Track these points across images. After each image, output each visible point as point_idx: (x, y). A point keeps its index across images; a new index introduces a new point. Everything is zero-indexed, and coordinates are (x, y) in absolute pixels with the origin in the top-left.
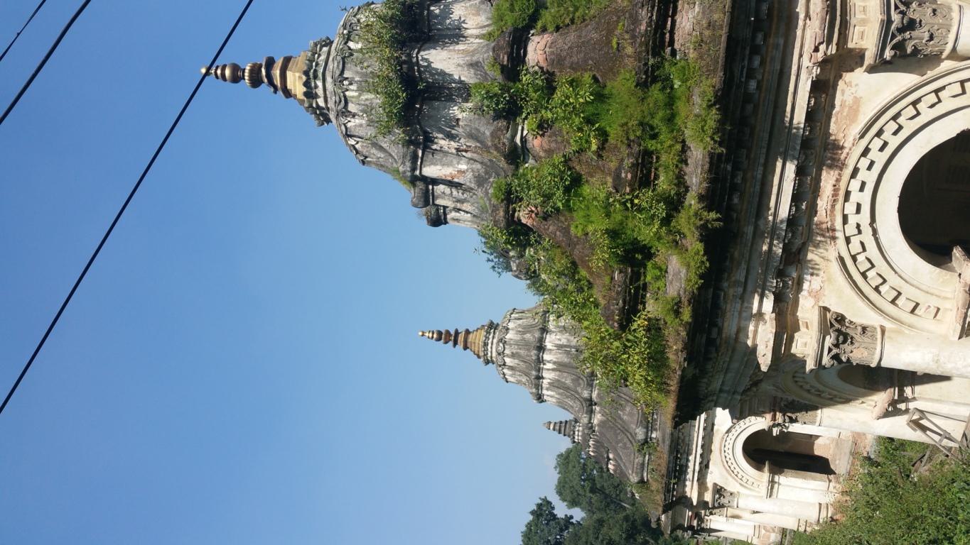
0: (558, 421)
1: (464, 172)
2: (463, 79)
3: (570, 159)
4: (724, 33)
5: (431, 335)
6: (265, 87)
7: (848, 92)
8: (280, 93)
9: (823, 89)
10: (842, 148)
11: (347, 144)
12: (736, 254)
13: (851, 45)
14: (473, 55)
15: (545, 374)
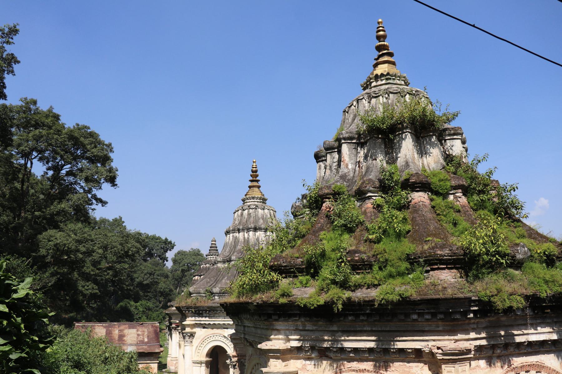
0: (217, 245)
1: (347, 167)
2: (399, 159)
3: (362, 225)
4: (441, 296)
6: (376, 54)
8: (375, 62)
10: (386, 371)
11: (353, 101)
12: (320, 323)
14: (412, 163)
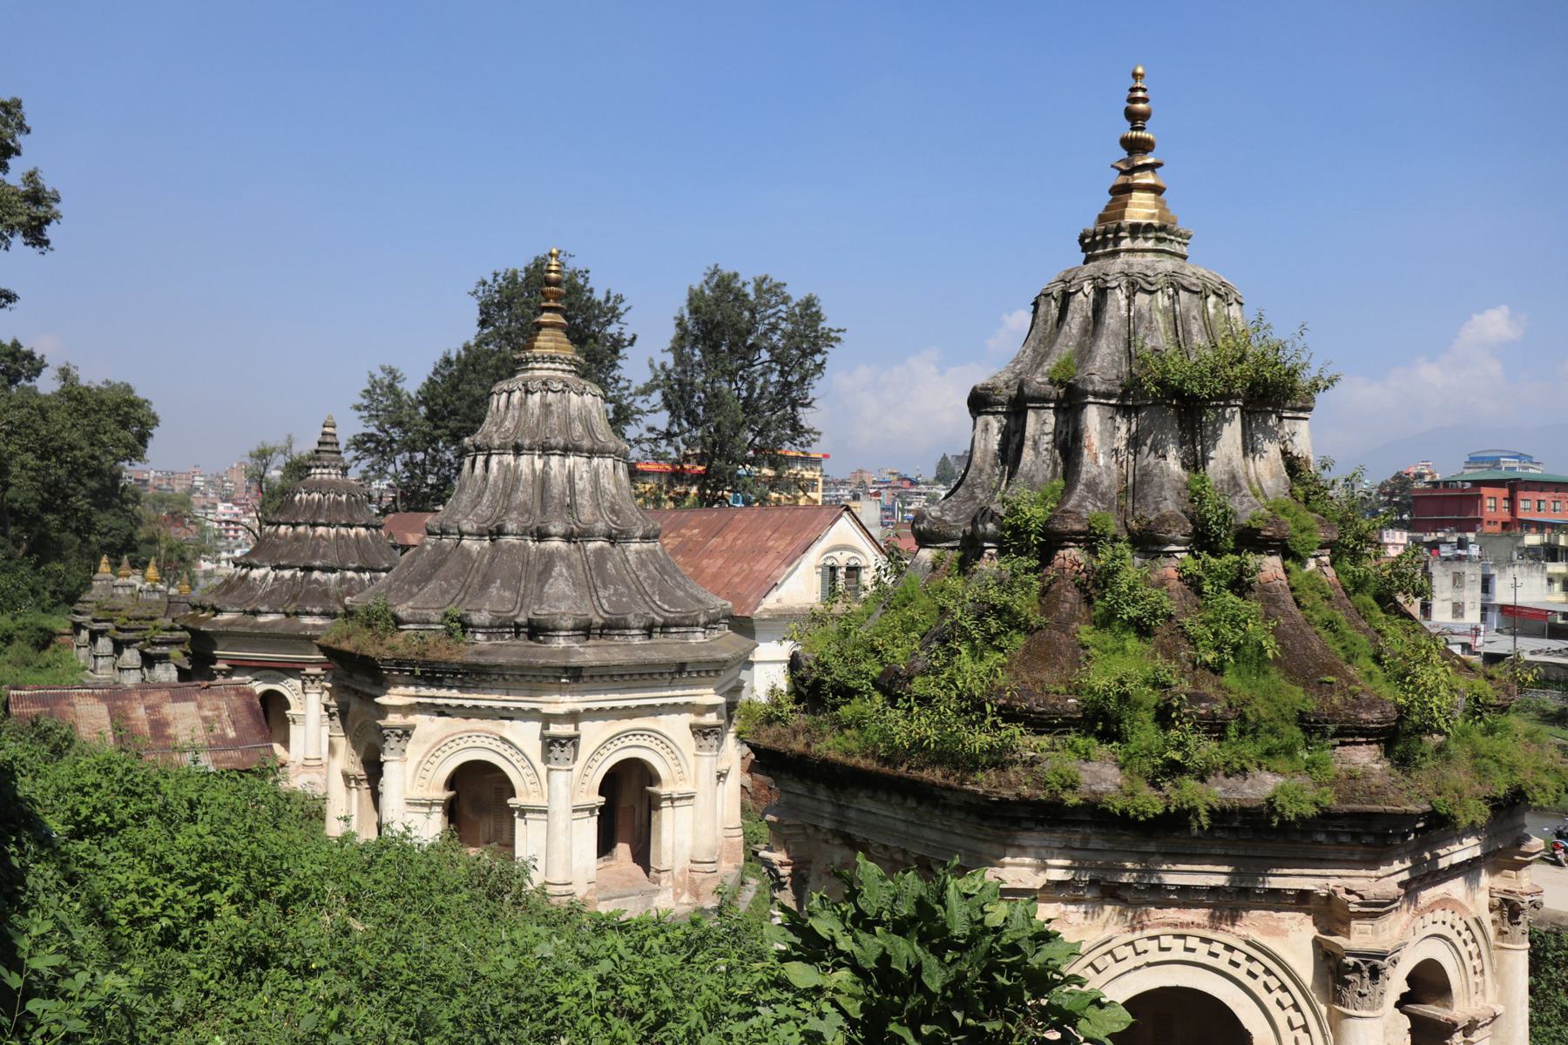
7: (1292, 923)
8: (1121, 180)
9: (1302, 900)
13: (1353, 923)
15: (524, 460)
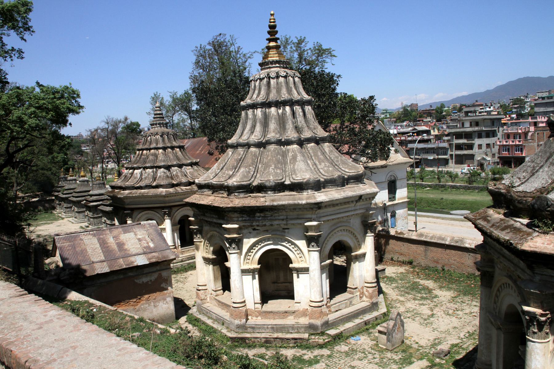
5: (272, 21)
